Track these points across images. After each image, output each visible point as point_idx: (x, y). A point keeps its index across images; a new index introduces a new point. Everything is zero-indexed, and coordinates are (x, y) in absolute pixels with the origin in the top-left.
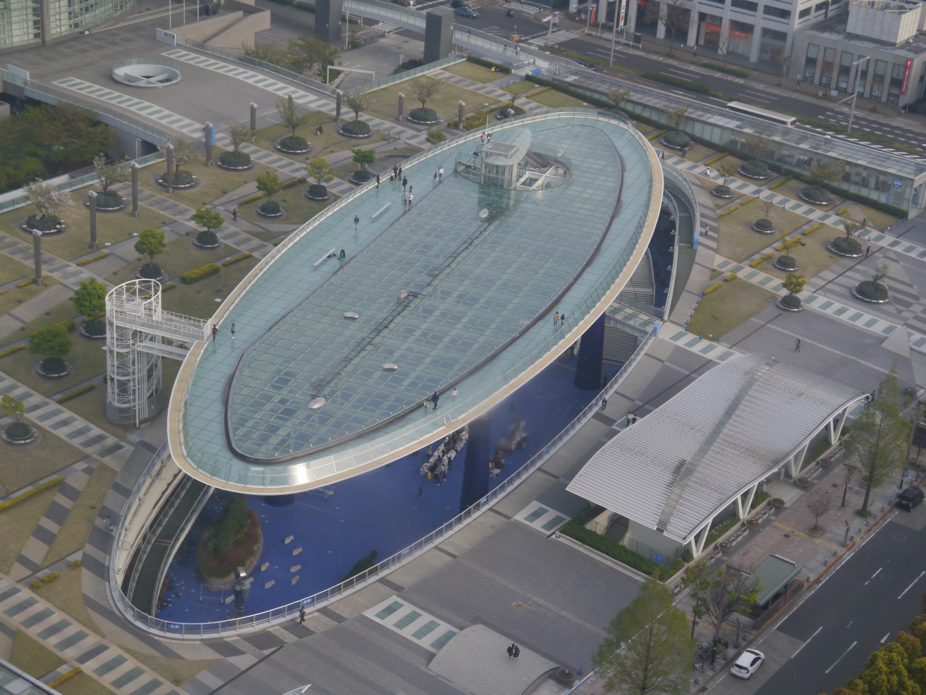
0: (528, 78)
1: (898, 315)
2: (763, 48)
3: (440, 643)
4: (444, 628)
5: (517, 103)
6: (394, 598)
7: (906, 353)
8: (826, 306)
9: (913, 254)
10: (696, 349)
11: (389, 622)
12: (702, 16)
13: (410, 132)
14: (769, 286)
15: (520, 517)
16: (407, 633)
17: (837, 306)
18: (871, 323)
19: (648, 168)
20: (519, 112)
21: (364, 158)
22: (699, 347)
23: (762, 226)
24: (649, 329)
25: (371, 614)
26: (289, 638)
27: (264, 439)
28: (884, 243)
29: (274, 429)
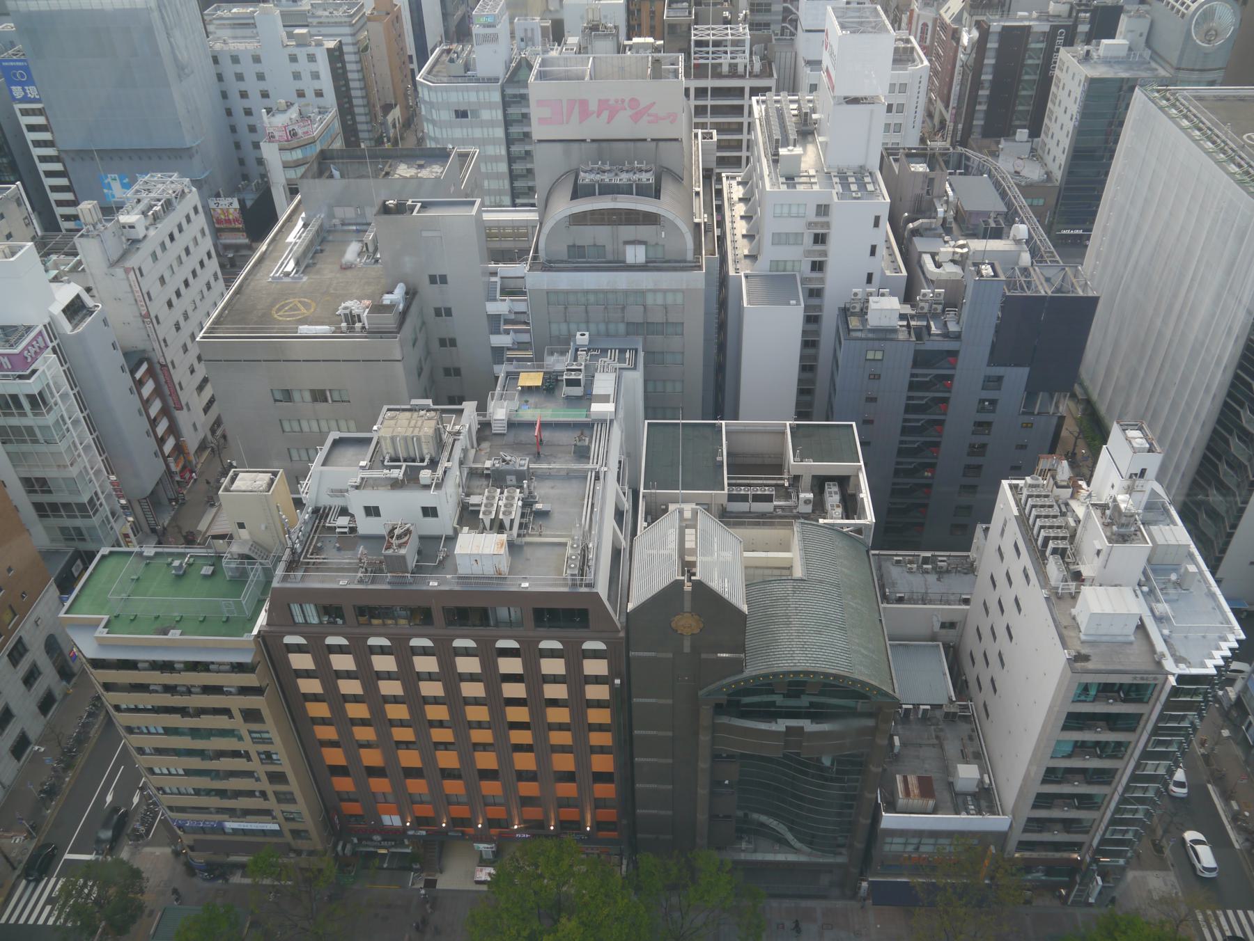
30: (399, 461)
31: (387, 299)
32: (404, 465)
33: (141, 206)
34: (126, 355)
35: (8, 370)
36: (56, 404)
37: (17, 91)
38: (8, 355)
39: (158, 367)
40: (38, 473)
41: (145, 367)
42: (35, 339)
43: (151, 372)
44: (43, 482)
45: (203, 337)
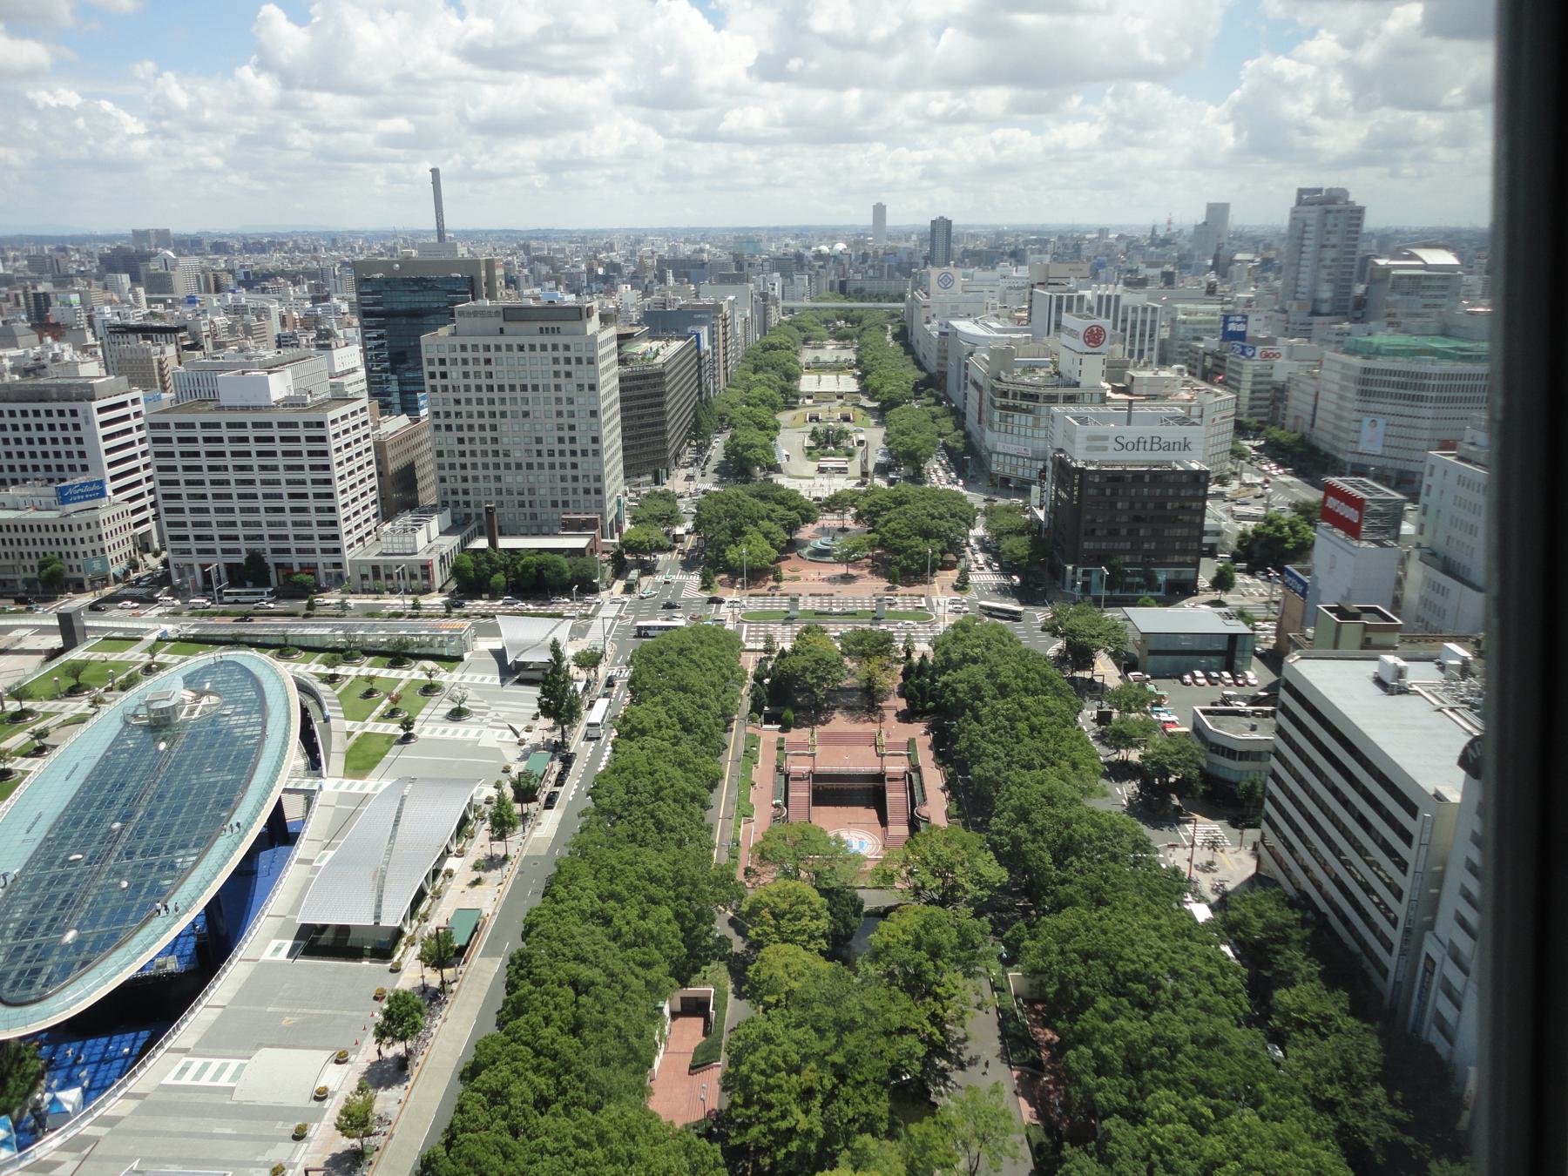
0: (159, 640)
1: (481, 722)
2: (327, 575)
3: (235, 1077)
4: (234, 1064)
5: (156, 659)
6: (185, 1060)
7: (497, 745)
8: (433, 731)
9: (477, 681)
10: (355, 790)
11: (187, 1080)
12: (278, 565)
13: (72, 705)
14: (390, 731)
15: (266, 956)
16: (205, 1081)
17: (441, 729)
18: (466, 733)
19: (279, 678)
20: (162, 666)
21: (41, 734)
22: (356, 786)
23: (369, 694)
24: (316, 787)
25: (169, 1080)
26: (101, 1131)
27: (30, 984)
28: (455, 680)
29: (36, 972)
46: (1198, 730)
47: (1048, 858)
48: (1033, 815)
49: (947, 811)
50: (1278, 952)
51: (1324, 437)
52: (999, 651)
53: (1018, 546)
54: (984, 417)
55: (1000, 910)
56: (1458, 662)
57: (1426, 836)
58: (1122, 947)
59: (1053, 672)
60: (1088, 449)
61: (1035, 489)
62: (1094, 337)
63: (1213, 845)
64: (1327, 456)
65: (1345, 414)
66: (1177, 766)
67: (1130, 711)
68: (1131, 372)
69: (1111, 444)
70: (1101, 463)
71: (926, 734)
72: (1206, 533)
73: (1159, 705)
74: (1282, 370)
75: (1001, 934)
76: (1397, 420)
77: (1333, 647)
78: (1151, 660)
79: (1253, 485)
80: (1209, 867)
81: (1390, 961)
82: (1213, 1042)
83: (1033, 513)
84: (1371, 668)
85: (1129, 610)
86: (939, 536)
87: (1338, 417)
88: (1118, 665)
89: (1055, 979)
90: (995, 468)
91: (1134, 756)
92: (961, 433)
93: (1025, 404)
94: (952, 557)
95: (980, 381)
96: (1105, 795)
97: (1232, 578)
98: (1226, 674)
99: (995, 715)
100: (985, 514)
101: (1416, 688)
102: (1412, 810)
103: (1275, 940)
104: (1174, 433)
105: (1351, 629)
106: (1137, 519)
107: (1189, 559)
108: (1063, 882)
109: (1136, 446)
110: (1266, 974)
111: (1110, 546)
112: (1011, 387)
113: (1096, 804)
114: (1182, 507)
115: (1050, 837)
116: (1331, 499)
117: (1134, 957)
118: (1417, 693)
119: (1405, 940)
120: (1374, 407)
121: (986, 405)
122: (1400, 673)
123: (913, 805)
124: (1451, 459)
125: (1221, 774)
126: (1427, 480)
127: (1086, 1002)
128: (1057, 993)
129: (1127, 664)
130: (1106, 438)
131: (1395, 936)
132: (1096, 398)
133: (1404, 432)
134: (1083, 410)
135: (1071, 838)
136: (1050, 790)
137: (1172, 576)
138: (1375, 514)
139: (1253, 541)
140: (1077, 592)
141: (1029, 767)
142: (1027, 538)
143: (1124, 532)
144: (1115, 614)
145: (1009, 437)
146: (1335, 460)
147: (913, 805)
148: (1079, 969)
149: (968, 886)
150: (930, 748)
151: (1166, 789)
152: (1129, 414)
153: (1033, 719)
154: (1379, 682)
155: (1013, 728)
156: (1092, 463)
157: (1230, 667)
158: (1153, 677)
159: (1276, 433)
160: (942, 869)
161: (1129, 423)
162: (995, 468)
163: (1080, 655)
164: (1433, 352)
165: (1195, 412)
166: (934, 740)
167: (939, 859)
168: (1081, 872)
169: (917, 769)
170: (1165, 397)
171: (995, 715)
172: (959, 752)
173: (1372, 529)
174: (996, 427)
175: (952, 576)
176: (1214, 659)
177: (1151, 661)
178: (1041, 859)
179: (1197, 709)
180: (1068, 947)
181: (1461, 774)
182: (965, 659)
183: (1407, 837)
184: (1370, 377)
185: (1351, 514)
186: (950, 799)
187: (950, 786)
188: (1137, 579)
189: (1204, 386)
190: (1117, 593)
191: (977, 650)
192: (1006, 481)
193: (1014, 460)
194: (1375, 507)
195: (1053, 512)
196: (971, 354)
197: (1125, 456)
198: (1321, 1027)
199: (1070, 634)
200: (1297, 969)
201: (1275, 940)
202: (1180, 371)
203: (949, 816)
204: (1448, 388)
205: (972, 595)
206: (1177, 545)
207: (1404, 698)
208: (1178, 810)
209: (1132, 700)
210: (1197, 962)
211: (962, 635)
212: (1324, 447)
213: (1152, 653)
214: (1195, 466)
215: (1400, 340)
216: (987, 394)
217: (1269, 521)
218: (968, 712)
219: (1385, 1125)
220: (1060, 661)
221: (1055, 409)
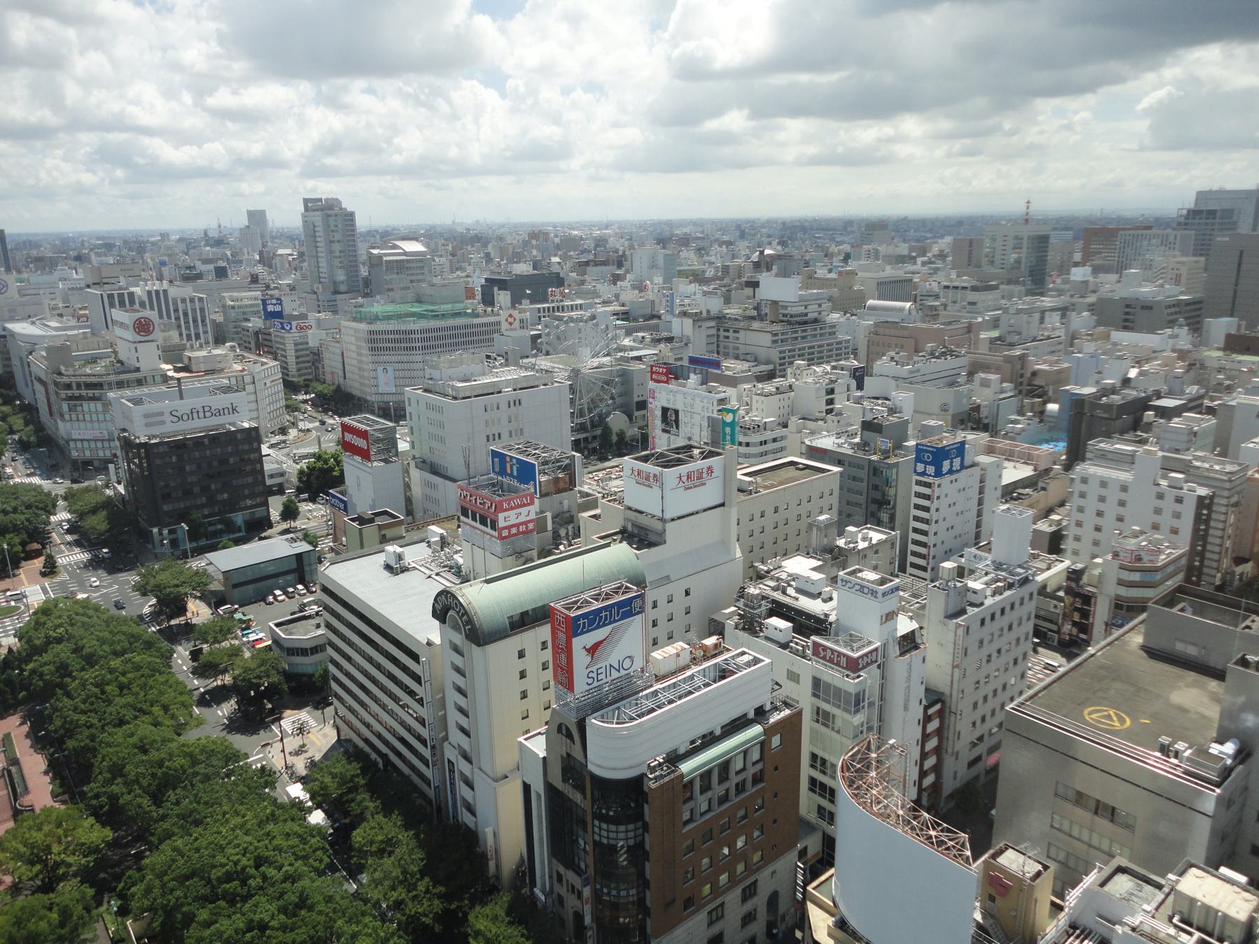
30: (1191, 925)
31: (1215, 749)
32: (1197, 935)
33: (986, 579)
34: (927, 690)
35: (842, 667)
36: (863, 707)
37: (920, 467)
38: (848, 657)
39: (947, 710)
40: (820, 753)
41: (938, 706)
42: (871, 652)
43: (941, 714)
44: (824, 762)
45: (1013, 709)
46: (277, 641)
47: (146, 802)
48: (128, 768)
49: (52, 792)
50: (353, 800)
51: (355, 386)
52: (84, 624)
53: (98, 522)
54: (55, 408)
55: (112, 867)
56: (438, 539)
57: (427, 674)
58: (214, 857)
59: (136, 630)
60: (147, 425)
61: (111, 466)
62: (143, 327)
63: (301, 730)
64: (359, 399)
65: (365, 366)
66: (260, 678)
67: (219, 642)
68: (188, 353)
69: (168, 418)
70: (162, 436)
71: (21, 724)
72: (271, 476)
73: (248, 628)
74: (314, 338)
75: (113, 890)
76: (400, 366)
77: (362, 549)
78: (237, 591)
79: (308, 430)
80: (300, 751)
81: (428, 773)
82: (303, 902)
83: (115, 488)
84: (380, 559)
85: (211, 556)
86: (16, 529)
87: (360, 369)
88: (209, 605)
89: (160, 912)
90: (74, 454)
91: (228, 679)
92: (31, 427)
93: (90, 393)
94: (36, 546)
95: (44, 378)
96: (200, 722)
97: (297, 508)
98: (300, 587)
99: (83, 685)
100: (65, 498)
101: (413, 565)
102: (415, 658)
103: (350, 791)
104: (222, 401)
105: (370, 531)
106: (211, 477)
107: (258, 500)
108: (163, 818)
109: (192, 414)
110: (347, 821)
111: (188, 503)
112: (73, 379)
113: (191, 736)
114: (242, 460)
115: (145, 782)
116: (346, 434)
117: (224, 860)
118: (415, 568)
119: (433, 755)
120: (382, 358)
121: (53, 398)
122: (400, 557)
123: (16, 800)
124: (420, 392)
125: (301, 670)
126: (408, 410)
127: (189, 919)
128: (163, 924)
129: (216, 600)
130: (162, 414)
131: (427, 753)
132: (158, 379)
133: (407, 374)
134: (138, 392)
135: (165, 774)
136: (141, 740)
137: (248, 517)
138: (378, 440)
139: (309, 475)
140: (167, 550)
141: (121, 723)
142: (104, 513)
143: (196, 490)
144: (197, 564)
145: (82, 424)
146: (366, 401)
147: (16, 800)
148: (178, 893)
149: (70, 860)
150: (27, 736)
151: (261, 696)
152: (180, 390)
153: (122, 679)
154: (388, 567)
155: (103, 692)
156: (155, 437)
157: (302, 581)
158: (240, 607)
159: (320, 388)
160: (37, 856)
161: (182, 398)
162: (74, 454)
163: (172, 605)
164: (413, 315)
165: (248, 379)
166: (31, 727)
167: (33, 846)
168: (178, 803)
169: (15, 762)
170: (222, 370)
171: (83, 685)
172: (56, 731)
173: (379, 452)
174: (67, 417)
175: (38, 563)
176: (289, 577)
177: (237, 593)
178: (140, 806)
179: (271, 624)
180: (166, 878)
181: (437, 623)
182: (49, 641)
183: (417, 679)
184: (375, 337)
185: (360, 443)
186: (53, 781)
187: (54, 768)
188: (219, 527)
189: (253, 357)
190: (203, 542)
191: (61, 630)
192: (87, 463)
193: (93, 444)
194: (377, 434)
195: (130, 485)
196: (31, 353)
197: (182, 426)
198: (385, 849)
199: (157, 590)
200: (367, 808)
201: (350, 791)
202: (233, 348)
203: (54, 795)
204: (428, 339)
205: (63, 577)
206: (246, 492)
207: (406, 574)
208: (272, 712)
209: (222, 630)
210: (279, 841)
211: (43, 619)
212: (355, 392)
213: (236, 586)
214: (246, 425)
215: (390, 308)
216: (52, 388)
217: (318, 457)
218: (59, 691)
219: (436, 902)
220: (155, 616)
221: (111, 395)
